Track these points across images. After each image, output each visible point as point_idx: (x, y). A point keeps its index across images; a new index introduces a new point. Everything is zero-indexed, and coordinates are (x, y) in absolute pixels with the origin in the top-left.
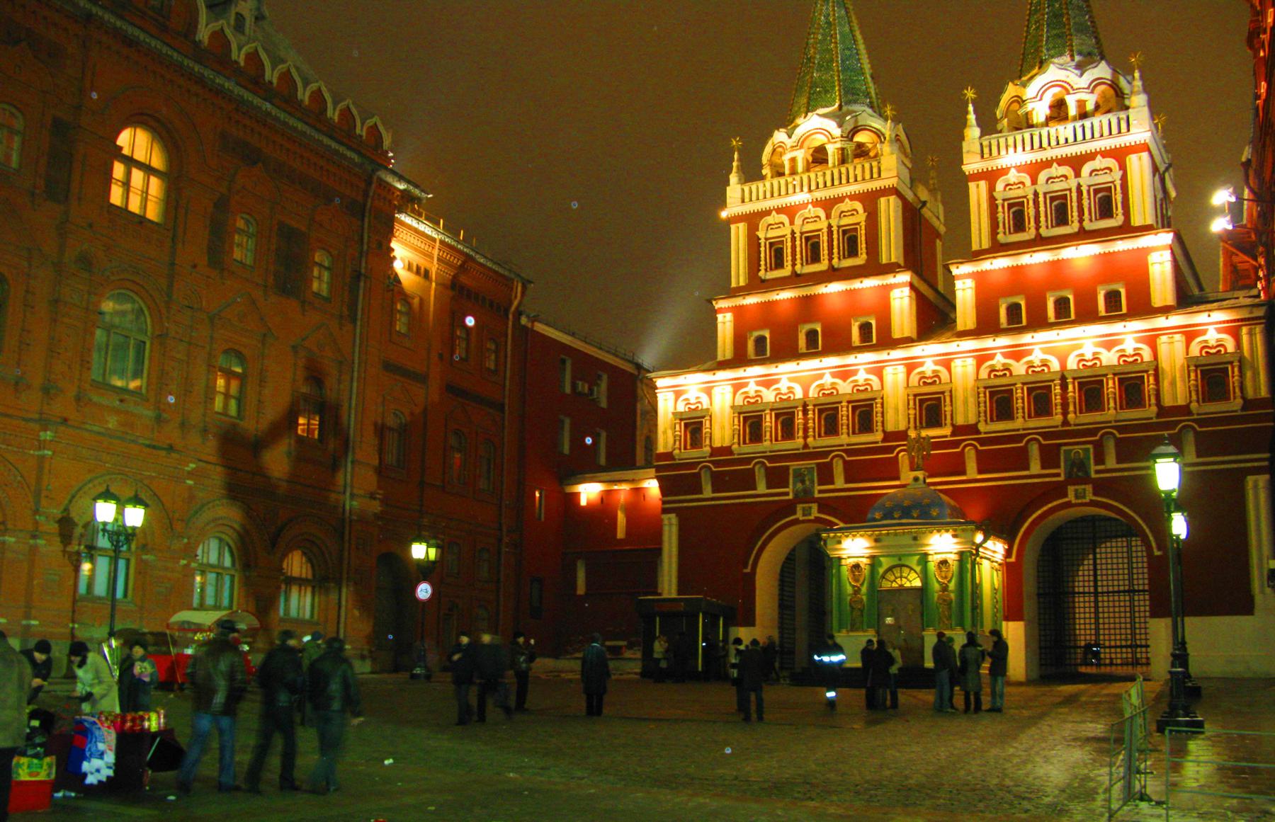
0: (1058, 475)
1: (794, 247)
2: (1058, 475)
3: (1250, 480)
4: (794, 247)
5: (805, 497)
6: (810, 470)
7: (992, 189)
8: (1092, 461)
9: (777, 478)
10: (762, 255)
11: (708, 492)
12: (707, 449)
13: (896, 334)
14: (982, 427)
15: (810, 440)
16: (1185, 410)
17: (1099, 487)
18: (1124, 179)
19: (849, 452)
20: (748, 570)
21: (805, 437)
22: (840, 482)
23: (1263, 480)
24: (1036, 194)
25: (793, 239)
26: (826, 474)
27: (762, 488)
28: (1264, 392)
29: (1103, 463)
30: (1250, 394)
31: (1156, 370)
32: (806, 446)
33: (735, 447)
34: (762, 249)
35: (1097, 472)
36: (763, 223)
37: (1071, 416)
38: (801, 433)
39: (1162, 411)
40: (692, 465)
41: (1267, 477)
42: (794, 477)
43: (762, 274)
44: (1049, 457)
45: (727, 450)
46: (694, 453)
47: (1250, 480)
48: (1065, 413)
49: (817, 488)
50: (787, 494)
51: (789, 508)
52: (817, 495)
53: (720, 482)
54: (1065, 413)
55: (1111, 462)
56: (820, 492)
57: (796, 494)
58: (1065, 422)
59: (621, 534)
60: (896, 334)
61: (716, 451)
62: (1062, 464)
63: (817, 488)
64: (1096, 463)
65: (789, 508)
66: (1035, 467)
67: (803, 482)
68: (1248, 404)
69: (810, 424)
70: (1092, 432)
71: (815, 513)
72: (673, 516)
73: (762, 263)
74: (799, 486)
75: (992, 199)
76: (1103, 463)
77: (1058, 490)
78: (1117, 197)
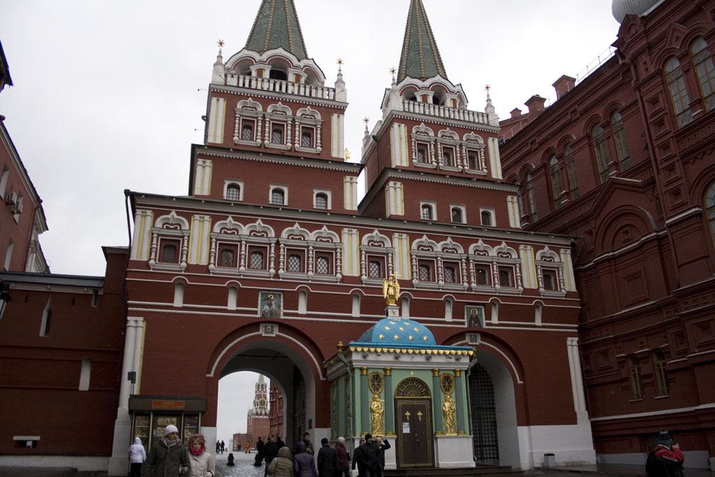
0: (463, 323)
1: (263, 127)
2: (463, 323)
4: (263, 127)
5: (269, 321)
7: (409, 132)
8: (484, 317)
9: (247, 298)
10: (237, 126)
11: (178, 301)
12: (184, 264)
14: (415, 281)
15: (281, 271)
16: (536, 292)
18: (486, 148)
19: (313, 286)
20: (212, 375)
21: (277, 269)
22: (302, 309)
24: (436, 141)
25: (264, 122)
26: (291, 303)
27: (232, 304)
28: (573, 289)
29: (491, 320)
31: (520, 264)
32: (277, 276)
33: (212, 266)
34: (237, 121)
35: (487, 324)
36: (239, 106)
37: (473, 285)
38: (272, 265)
40: (170, 276)
41: (577, 339)
42: (262, 300)
43: (236, 138)
44: (458, 313)
45: (206, 269)
48: (469, 282)
49: (282, 311)
50: (256, 312)
51: (255, 325)
52: (282, 317)
54: (469, 282)
55: (495, 320)
56: (285, 314)
57: (264, 314)
58: (470, 289)
62: (466, 316)
63: (282, 311)
64: (486, 320)
65: (255, 325)
66: (448, 317)
67: (270, 305)
68: (569, 294)
69: (281, 259)
70: (487, 297)
71: (276, 332)
72: (141, 319)
73: (236, 131)
74: (267, 307)
75: (409, 137)
76: (491, 320)
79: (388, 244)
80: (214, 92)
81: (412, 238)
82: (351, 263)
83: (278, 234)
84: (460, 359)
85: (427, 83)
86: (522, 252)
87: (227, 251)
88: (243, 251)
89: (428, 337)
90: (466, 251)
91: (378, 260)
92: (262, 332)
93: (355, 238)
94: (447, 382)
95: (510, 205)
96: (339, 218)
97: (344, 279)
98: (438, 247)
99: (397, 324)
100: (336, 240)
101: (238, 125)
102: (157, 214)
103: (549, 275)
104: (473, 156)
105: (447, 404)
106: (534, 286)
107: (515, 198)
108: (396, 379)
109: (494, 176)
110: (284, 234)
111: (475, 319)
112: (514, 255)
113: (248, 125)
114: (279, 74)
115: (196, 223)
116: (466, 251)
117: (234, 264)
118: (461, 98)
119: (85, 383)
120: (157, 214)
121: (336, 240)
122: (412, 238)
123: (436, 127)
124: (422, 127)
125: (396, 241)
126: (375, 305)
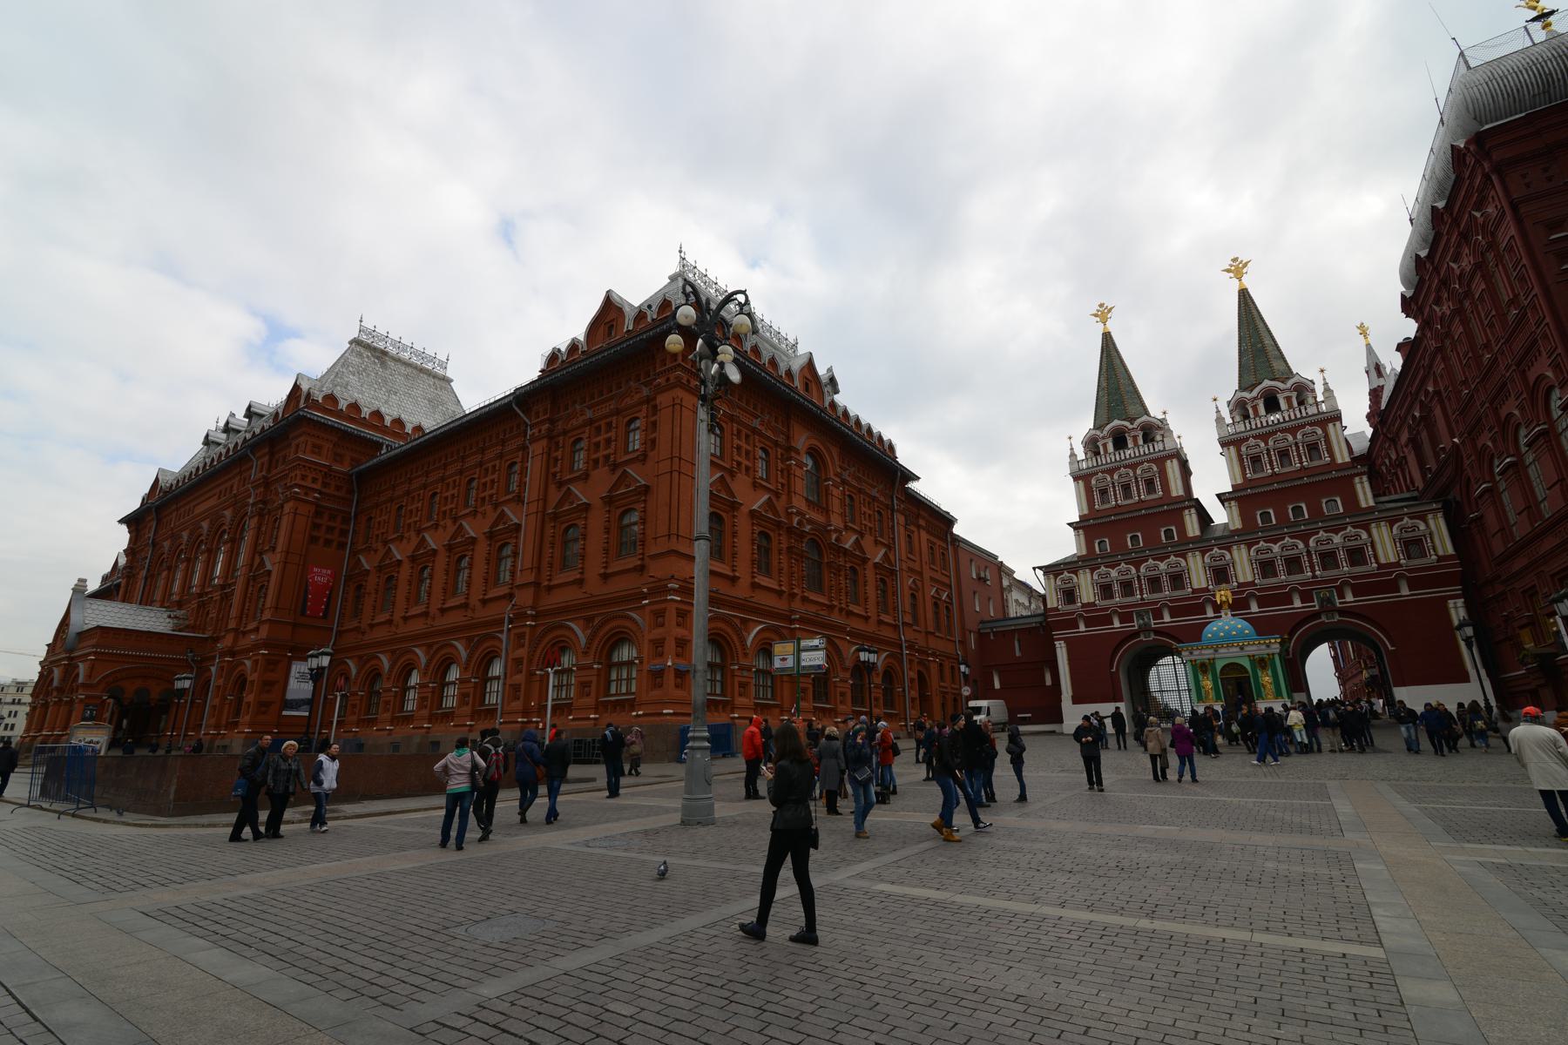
3: (1451, 603)
5: (1145, 629)
6: (1147, 612)
7: (1239, 451)
9: (1126, 618)
11: (1082, 628)
13: (1191, 534)
16: (1397, 564)
17: (1342, 612)
18: (1327, 436)
22: (1167, 618)
23: (1460, 602)
26: (1158, 614)
27: (1117, 624)
28: (1450, 550)
30: (1441, 553)
39: (1380, 566)
44: (1306, 597)
45: (1093, 604)
46: (1070, 607)
47: (1451, 603)
48: (1313, 571)
53: (1089, 622)
54: (1313, 571)
58: (1314, 576)
59: (1018, 654)
60: (1191, 534)
61: (1084, 605)
65: (1136, 634)
68: (1440, 559)
71: (1153, 636)
77: (1316, 615)
78: (1322, 446)
79: (1228, 557)
80: (1076, 479)
81: (1249, 547)
82: (1198, 577)
83: (1138, 570)
84: (1274, 645)
85: (1255, 393)
86: (1374, 531)
87: (1106, 590)
88: (1116, 587)
89: (1248, 629)
90: (1307, 545)
91: (1221, 574)
92: (1142, 638)
93: (1199, 558)
94: (1262, 663)
95: (1358, 487)
96: (1184, 546)
97: (1194, 591)
98: (1276, 548)
99: (1226, 624)
100: (1183, 563)
101: (1096, 496)
102: (1056, 577)
103: (1412, 545)
104: (1313, 448)
105: (1266, 679)
106: (1393, 559)
107: (1365, 478)
108: (1219, 665)
109: (1340, 461)
110: (1142, 570)
111: (1330, 600)
112: (1364, 536)
113: (1104, 492)
114: (1120, 441)
115: (1081, 576)
116: (1307, 545)
117: (1112, 597)
118: (1303, 390)
119: (1049, 682)
120: (1056, 577)
121: (1183, 563)
122: (1249, 547)
123: (1264, 437)
124: (1252, 441)
125: (1235, 553)
126: (1217, 608)
